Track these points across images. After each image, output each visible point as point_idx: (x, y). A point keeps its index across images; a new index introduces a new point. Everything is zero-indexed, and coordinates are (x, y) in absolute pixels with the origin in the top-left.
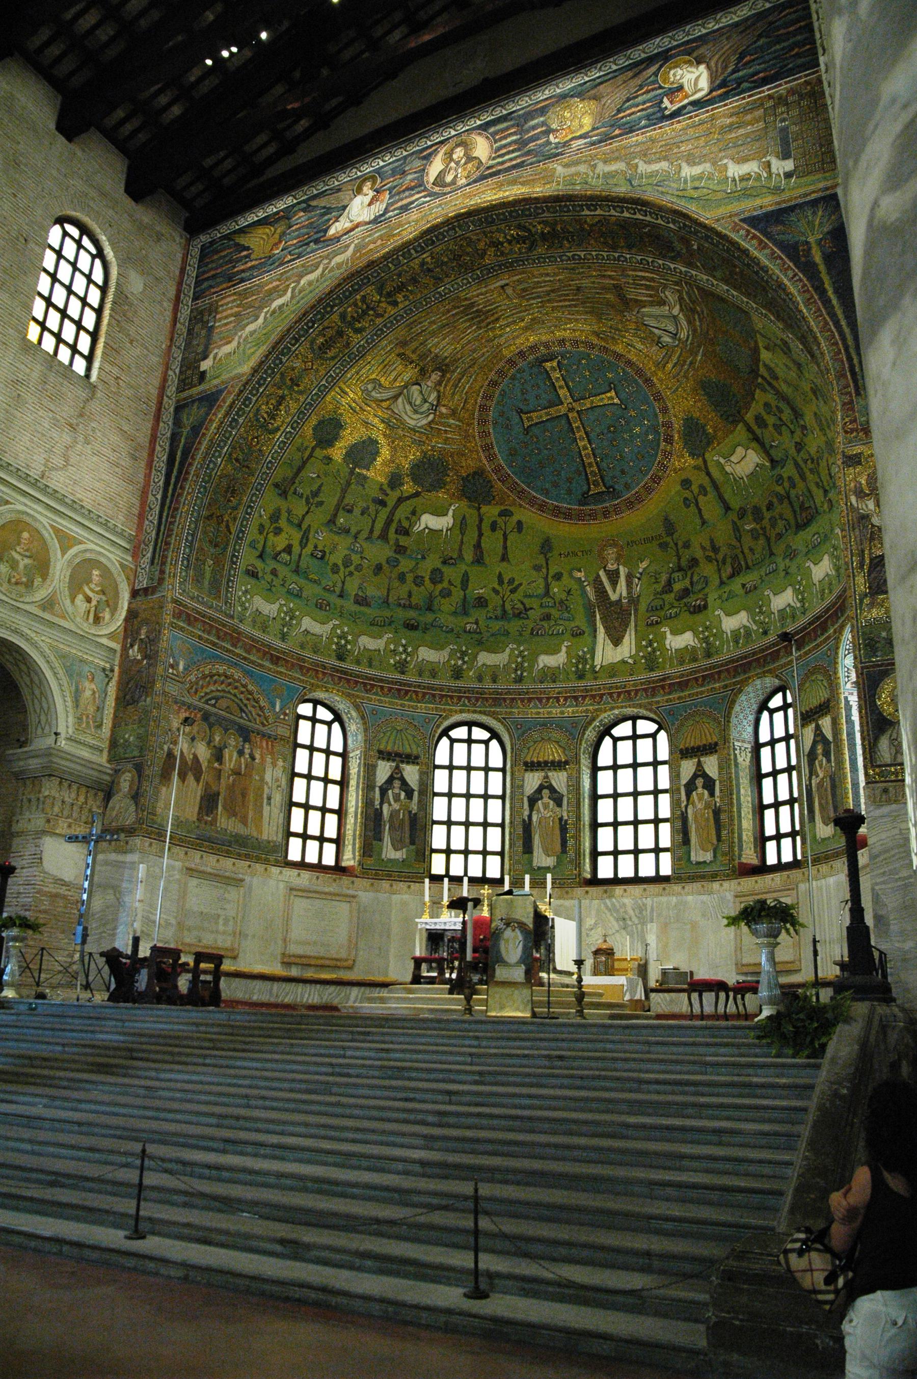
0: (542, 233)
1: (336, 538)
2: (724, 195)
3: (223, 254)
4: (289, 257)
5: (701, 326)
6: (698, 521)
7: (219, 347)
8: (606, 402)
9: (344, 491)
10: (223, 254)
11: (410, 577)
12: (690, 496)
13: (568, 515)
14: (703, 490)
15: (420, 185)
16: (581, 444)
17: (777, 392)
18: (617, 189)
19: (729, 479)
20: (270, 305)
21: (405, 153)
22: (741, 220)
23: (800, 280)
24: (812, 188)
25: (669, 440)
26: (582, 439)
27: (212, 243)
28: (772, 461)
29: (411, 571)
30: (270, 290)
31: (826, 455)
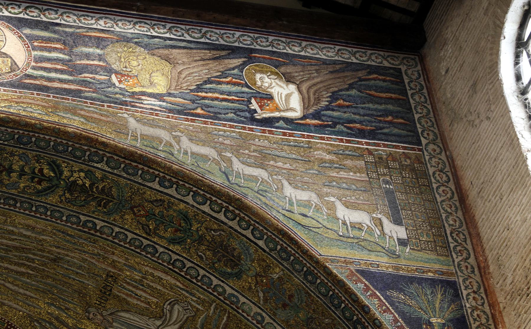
22: (357, 271)
24: (427, 265)
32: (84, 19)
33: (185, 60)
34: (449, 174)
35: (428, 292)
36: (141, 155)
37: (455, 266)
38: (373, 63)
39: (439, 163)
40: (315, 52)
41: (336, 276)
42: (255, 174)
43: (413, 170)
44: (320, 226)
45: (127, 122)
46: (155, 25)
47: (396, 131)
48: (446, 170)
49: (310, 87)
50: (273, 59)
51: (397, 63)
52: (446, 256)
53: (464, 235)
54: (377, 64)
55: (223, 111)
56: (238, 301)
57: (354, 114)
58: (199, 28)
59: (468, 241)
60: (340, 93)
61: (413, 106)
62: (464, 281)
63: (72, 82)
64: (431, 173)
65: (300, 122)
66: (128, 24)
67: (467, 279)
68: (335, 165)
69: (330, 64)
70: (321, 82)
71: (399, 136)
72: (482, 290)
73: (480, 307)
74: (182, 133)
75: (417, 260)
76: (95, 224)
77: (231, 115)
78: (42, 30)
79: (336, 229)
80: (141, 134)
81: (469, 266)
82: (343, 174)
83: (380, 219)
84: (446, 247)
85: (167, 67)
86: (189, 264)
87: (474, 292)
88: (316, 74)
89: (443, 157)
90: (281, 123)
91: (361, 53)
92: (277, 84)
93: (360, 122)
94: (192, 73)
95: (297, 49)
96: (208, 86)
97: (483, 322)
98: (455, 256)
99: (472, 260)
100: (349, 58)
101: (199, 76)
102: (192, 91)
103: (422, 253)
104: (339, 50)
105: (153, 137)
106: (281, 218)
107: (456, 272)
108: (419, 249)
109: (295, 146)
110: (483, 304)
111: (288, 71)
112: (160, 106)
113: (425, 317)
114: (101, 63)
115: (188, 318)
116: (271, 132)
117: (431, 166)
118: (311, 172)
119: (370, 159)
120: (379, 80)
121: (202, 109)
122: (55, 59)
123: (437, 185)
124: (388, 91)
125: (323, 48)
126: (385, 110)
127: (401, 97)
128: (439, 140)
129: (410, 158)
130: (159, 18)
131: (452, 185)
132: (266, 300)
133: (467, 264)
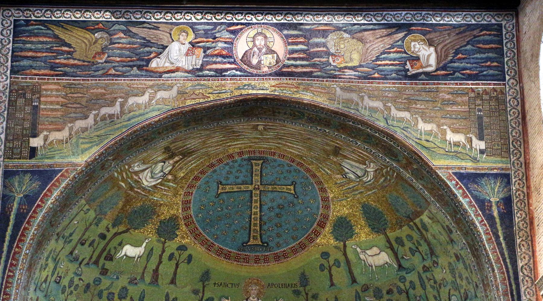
0: (311, 118)
1: (70, 265)
2: (445, 153)
3: (41, 39)
4: (113, 72)
5: (382, 183)
6: (329, 283)
7: (50, 131)
8: (285, 190)
9: (87, 229)
10: (41, 39)
11: (105, 294)
12: (326, 265)
13: (228, 256)
14: (337, 263)
15: (228, 56)
16: (254, 210)
17: (422, 236)
18: (378, 123)
19: (361, 263)
20: (99, 109)
21: (215, 21)
22: (453, 173)
23: (485, 225)
25: (322, 225)
26: (256, 207)
27: (28, 22)
28: (400, 266)
29: (107, 289)
30: (97, 95)
31: (449, 287)
32: (317, 17)
33: (371, 39)
34: (519, 100)
35: (492, 182)
36: (341, 113)
37: (511, 164)
38: (485, 22)
39: (514, 93)
40: (449, 19)
41: (441, 177)
42: (403, 116)
43: (497, 99)
44: (436, 146)
45: (336, 91)
46: (356, 15)
47: (491, 72)
48: (518, 97)
49: (443, 48)
50: (423, 30)
51: (500, 19)
52: (507, 158)
53: (520, 142)
54: (488, 23)
55: (390, 73)
56: (400, 170)
57: (467, 63)
58: (381, 12)
59: (522, 146)
60: (461, 49)
61: (505, 51)
62: (515, 173)
63: (308, 66)
64: (508, 100)
65: (433, 74)
66: (341, 17)
67: (517, 171)
68: (451, 102)
69: (457, 28)
70: (450, 43)
71: (493, 75)
72: (524, 178)
73: (521, 189)
74: (365, 93)
75: (489, 163)
76: (325, 131)
77: (394, 75)
78: (294, 30)
79: (444, 147)
80: (342, 99)
81: (519, 163)
82: (455, 108)
83: (471, 138)
84: (507, 152)
85: (360, 46)
86: (374, 151)
87: (520, 180)
88: (447, 37)
89: (518, 88)
90: (423, 76)
91: (478, 15)
92: (423, 48)
93: (470, 69)
94: (375, 48)
95: (438, 19)
96: (383, 56)
97: (521, 198)
98: (512, 157)
99: (522, 159)
100: (470, 21)
101: (378, 50)
102: (373, 61)
103: (492, 157)
104: (465, 15)
105: (348, 100)
106: (414, 144)
107: (511, 168)
108: (491, 154)
109: (429, 91)
110: (523, 187)
111: (431, 37)
112: (355, 75)
113: (488, 198)
114: (325, 49)
115: (378, 169)
116: (416, 84)
117: (509, 96)
118: (436, 109)
119: (472, 95)
120: (487, 35)
121: (378, 74)
122: (300, 50)
123: (510, 109)
124: (491, 42)
125: (455, 15)
126: (486, 58)
127: (499, 46)
128: (517, 76)
129: (496, 91)
130: (359, 8)
131: (519, 108)
132: (412, 174)
133: (518, 162)
